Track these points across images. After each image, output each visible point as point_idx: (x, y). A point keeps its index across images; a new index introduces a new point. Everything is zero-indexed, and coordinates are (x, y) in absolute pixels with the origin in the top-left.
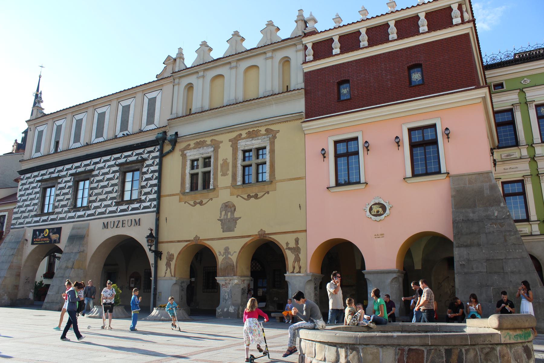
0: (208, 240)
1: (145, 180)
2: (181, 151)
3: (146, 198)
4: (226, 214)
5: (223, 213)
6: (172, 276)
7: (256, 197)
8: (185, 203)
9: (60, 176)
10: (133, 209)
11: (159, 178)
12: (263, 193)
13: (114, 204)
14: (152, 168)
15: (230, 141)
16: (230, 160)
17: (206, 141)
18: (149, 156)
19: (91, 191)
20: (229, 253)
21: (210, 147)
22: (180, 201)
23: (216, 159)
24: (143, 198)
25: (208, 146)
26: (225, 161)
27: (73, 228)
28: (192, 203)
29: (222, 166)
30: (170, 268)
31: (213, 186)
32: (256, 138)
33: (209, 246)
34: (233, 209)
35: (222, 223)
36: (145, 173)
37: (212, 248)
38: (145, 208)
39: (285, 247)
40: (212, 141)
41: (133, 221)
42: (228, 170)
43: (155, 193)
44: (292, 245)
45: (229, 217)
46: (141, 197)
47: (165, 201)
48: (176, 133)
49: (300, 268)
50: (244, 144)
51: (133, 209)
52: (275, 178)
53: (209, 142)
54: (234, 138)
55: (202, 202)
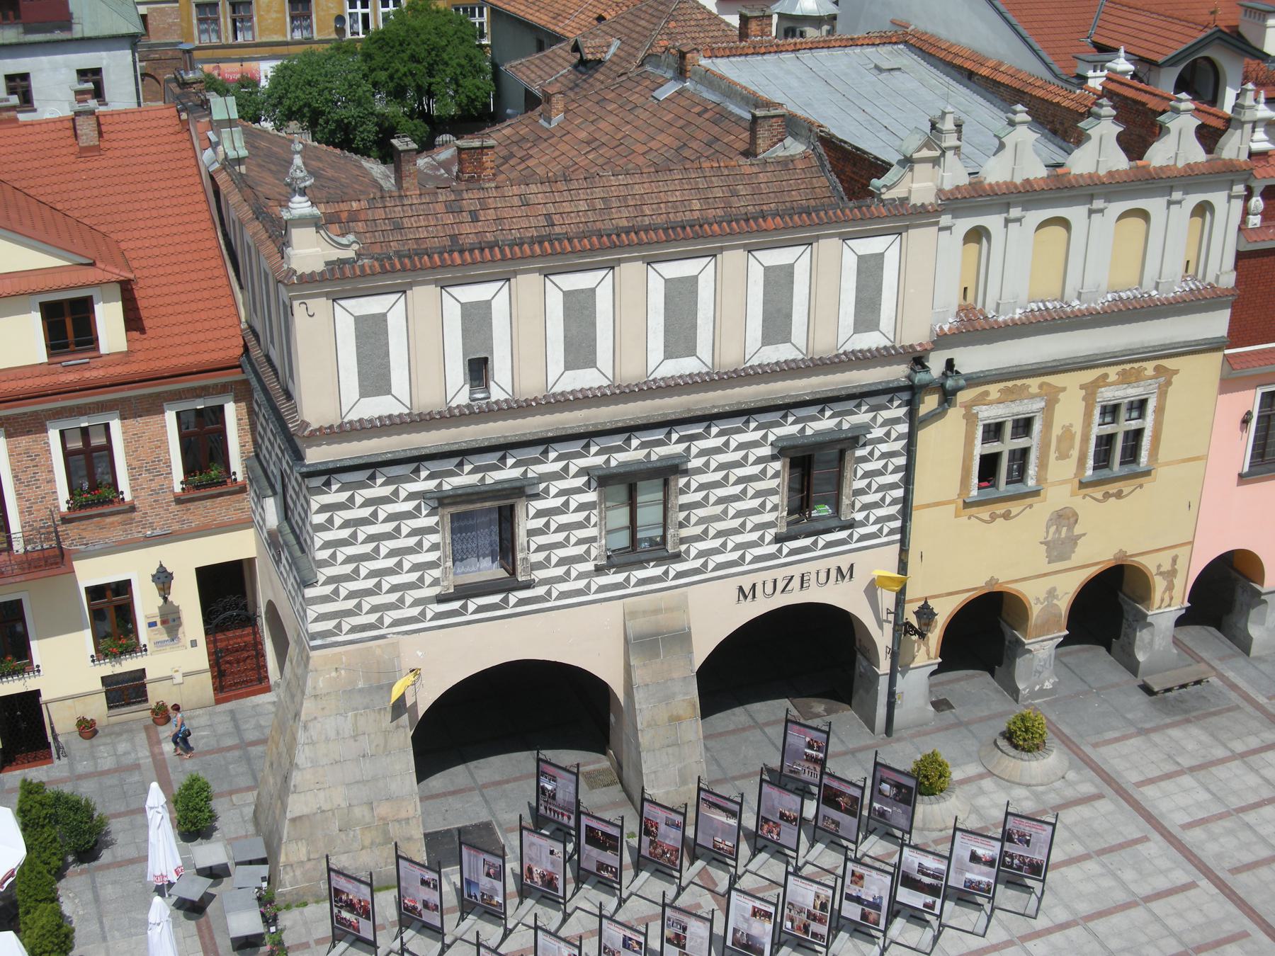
0: (1016, 581)
1: (863, 477)
2: (965, 407)
3: (867, 518)
4: (1058, 531)
5: (1053, 529)
6: (929, 658)
7: (1119, 495)
8: (969, 518)
9: (530, 475)
10: (829, 545)
11: (909, 469)
12: (1133, 488)
13: (768, 538)
14: (884, 448)
15: (1082, 387)
16: (1078, 429)
17: (1029, 386)
18: (875, 417)
19: (682, 515)
20: (1056, 597)
21: (1038, 399)
22: (957, 516)
23: (1048, 425)
24: (859, 516)
25: (1033, 397)
26: (1067, 430)
27: (629, 615)
28: (986, 516)
29: (1059, 439)
30: (927, 645)
31: (1038, 481)
32: (1135, 385)
33: (1017, 591)
34: (1072, 520)
35: (1048, 547)
36: (864, 459)
37: (1024, 595)
38: (863, 538)
39: (1154, 571)
40: (1041, 386)
41: (833, 573)
42: (1072, 447)
43: (894, 502)
44: (1166, 567)
45: (1063, 534)
46: (853, 516)
47: (919, 519)
48: (950, 364)
49: (1171, 599)
50: (1109, 394)
51: (829, 545)
52: (1157, 460)
53: (1034, 389)
54: (1092, 383)
55: (1009, 512)
